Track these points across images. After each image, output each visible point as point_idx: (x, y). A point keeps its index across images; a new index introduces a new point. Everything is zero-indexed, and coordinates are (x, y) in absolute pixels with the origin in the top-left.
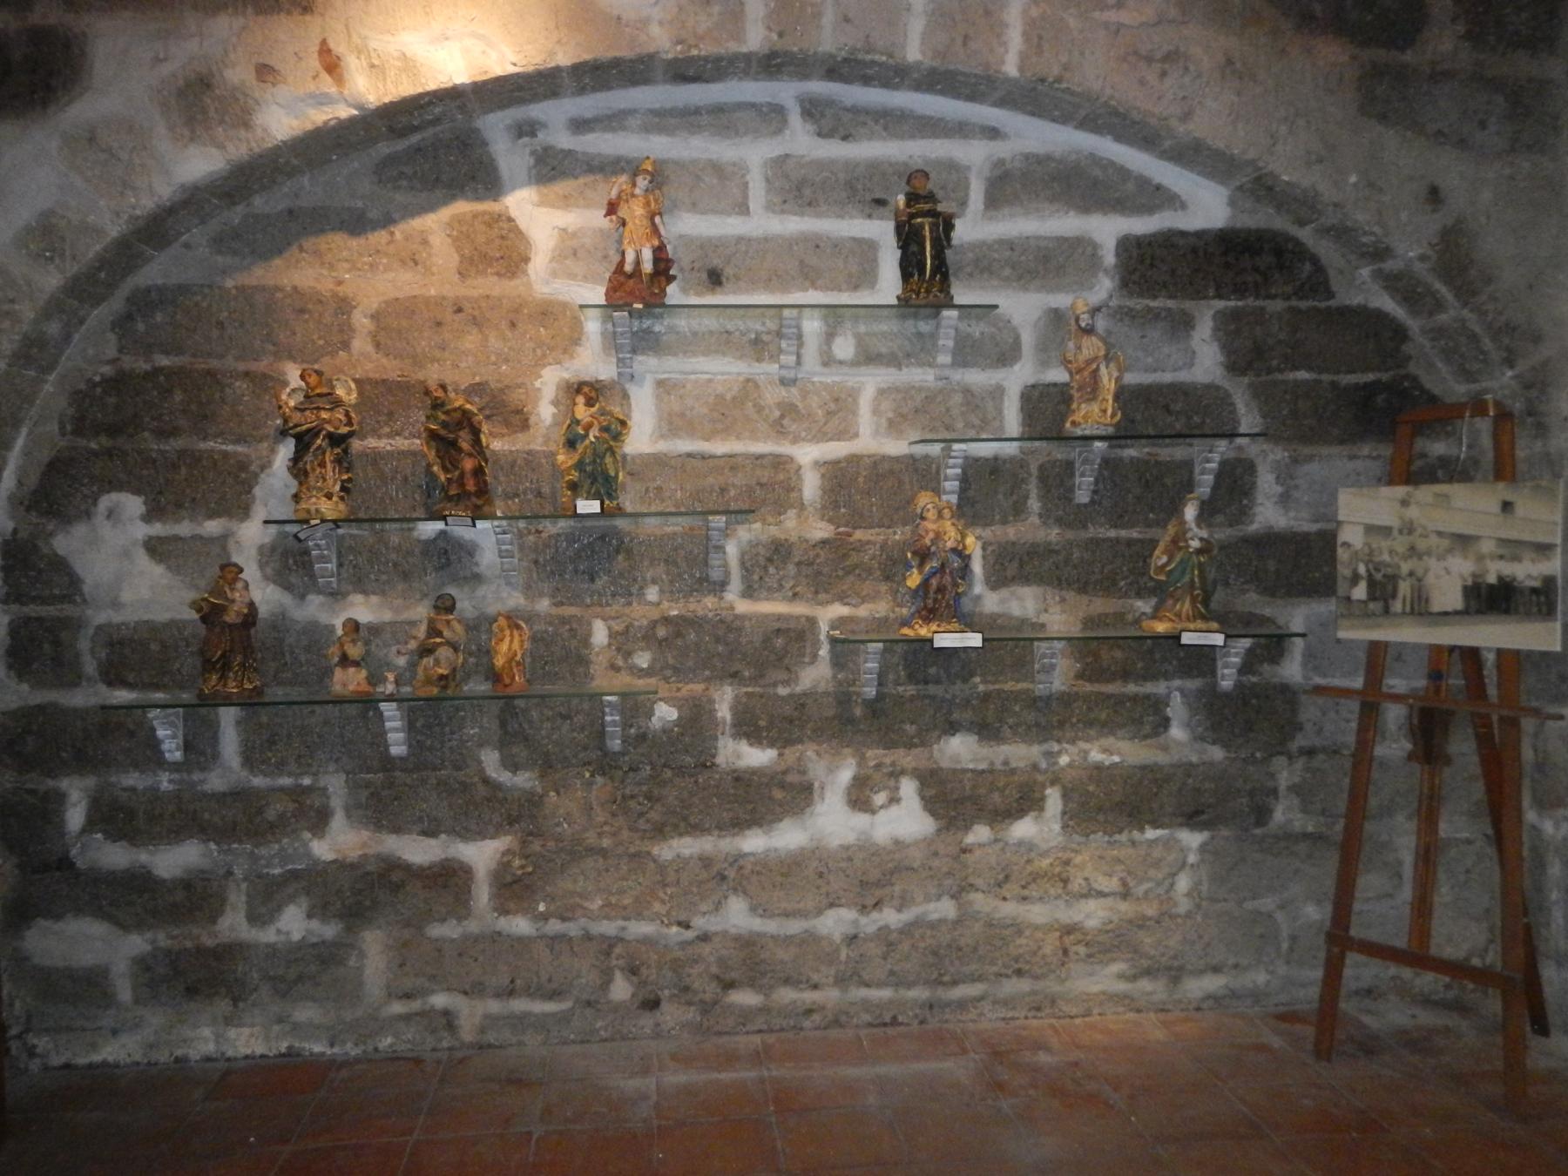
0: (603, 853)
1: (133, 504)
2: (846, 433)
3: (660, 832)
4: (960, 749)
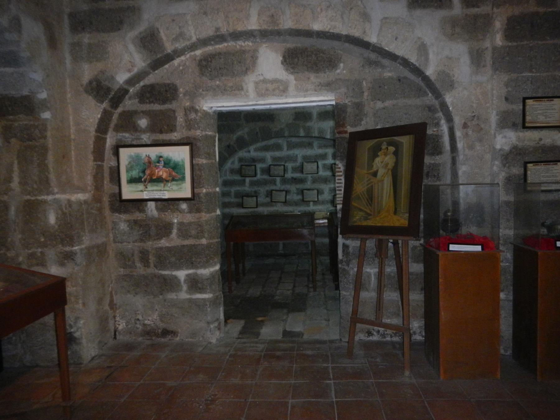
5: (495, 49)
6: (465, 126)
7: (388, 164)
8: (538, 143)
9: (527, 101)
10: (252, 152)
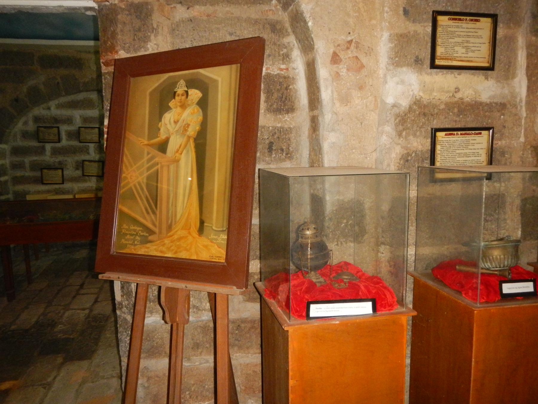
6: (335, 59)
7: (188, 125)
8: (453, 96)
9: (440, 18)
10: (53, 109)
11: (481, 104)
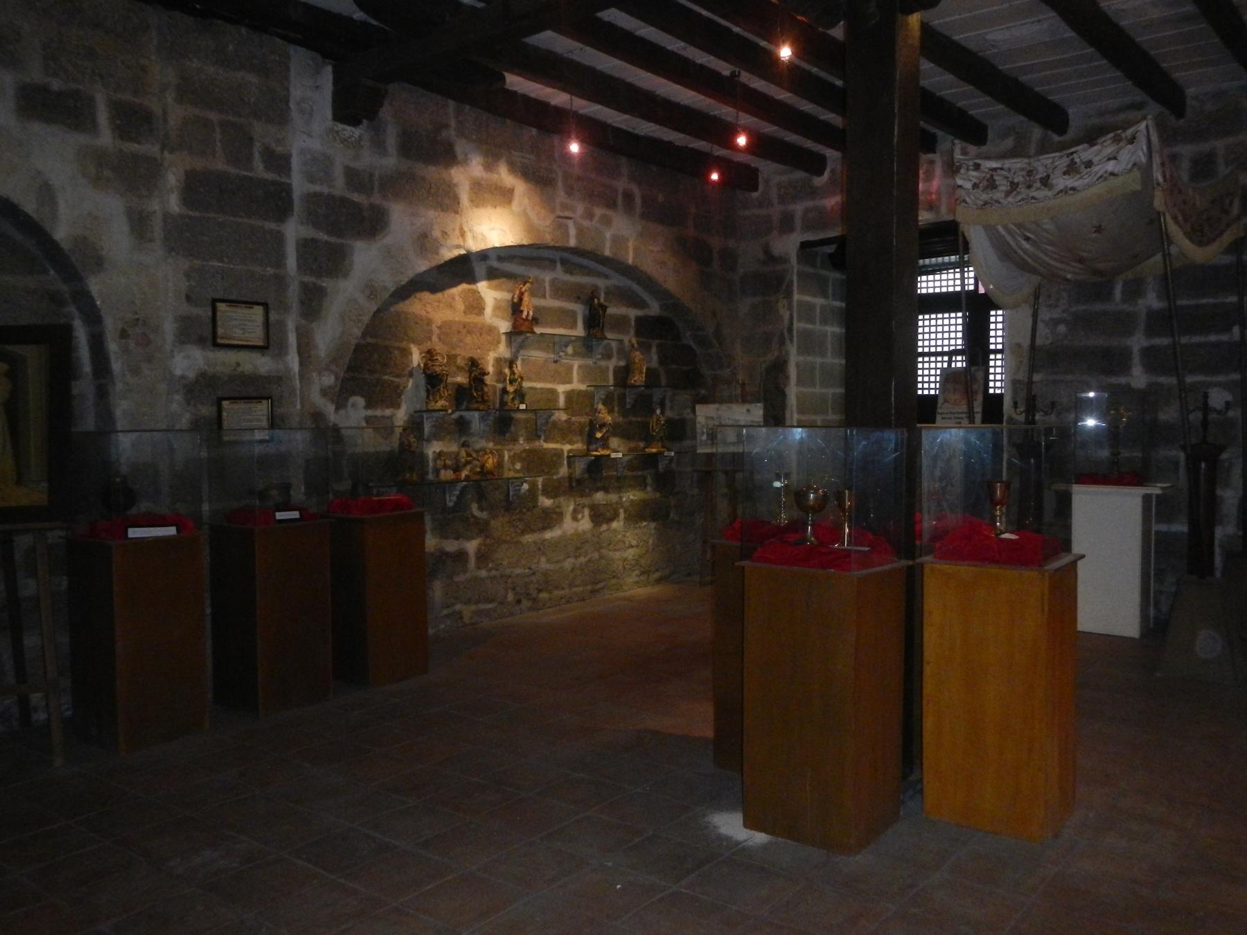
0: (505, 542)
1: (360, 401)
2: (570, 382)
3: (523, 532)
4: (599, 497)
5: (167, 216)
6: (124, 334)
9: (219, 304)
11: (261, 376)
